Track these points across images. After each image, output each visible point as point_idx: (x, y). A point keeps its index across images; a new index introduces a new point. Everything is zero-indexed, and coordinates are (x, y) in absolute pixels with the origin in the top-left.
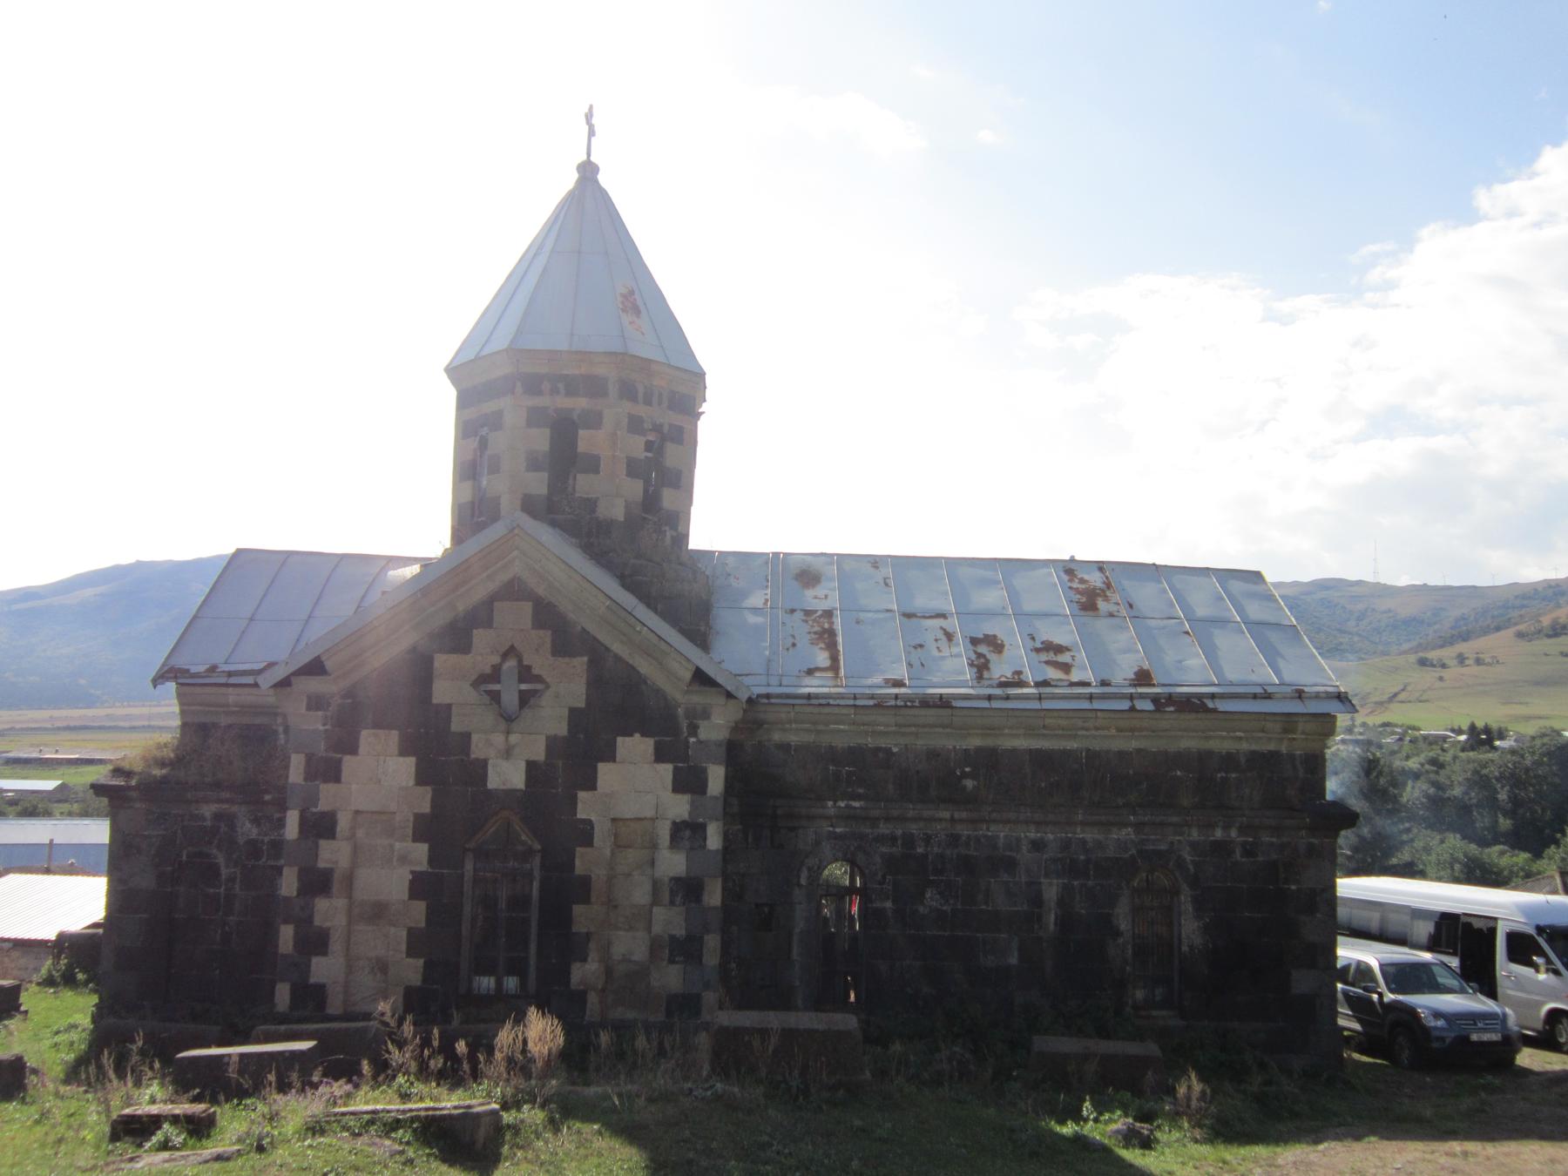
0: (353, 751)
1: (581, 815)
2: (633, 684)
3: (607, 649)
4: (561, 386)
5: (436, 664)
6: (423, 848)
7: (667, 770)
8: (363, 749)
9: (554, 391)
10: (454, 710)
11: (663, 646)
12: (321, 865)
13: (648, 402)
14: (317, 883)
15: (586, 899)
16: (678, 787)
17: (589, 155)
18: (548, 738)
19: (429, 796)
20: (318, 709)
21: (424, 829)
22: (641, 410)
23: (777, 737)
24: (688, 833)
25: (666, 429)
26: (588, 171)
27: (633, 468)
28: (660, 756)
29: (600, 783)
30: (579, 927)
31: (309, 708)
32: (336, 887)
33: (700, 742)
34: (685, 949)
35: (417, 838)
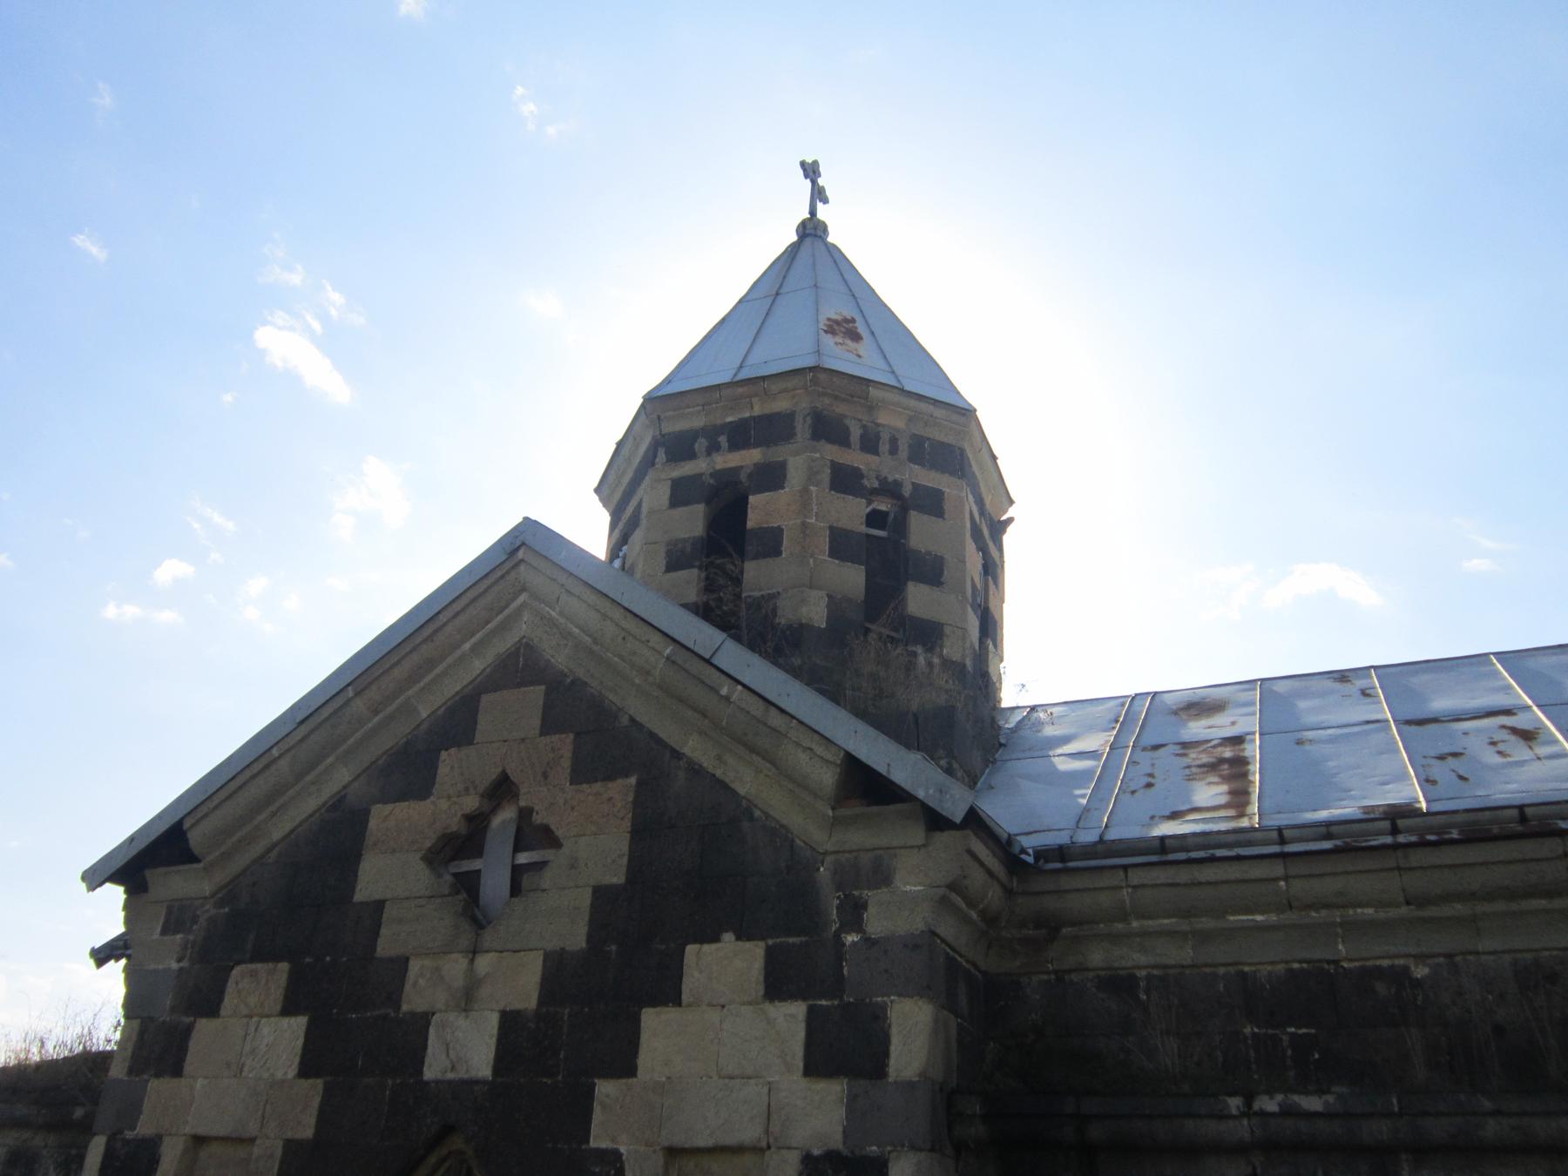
0: (212, 1010)
1: (598, 1140)
2: (723, 817)
3: (676, 755)
4: (723, 440)
5: (373, 823)
7: (791, 1016)
8: (229, 1002)
9: (713, 448)
10: (389, 912)
11: (776, 720)
13: (870, 444)
16: (818, 1064)
18: (548, 956)
19: (316, 1102)
20: (176, 932)
22: (855, 458)
23: (1097, 957)
25: (907, 491)
26: (811, 230)
27: (842, 546)
28: (779, 983)
29: (644, 1060)
33: (869, 942)
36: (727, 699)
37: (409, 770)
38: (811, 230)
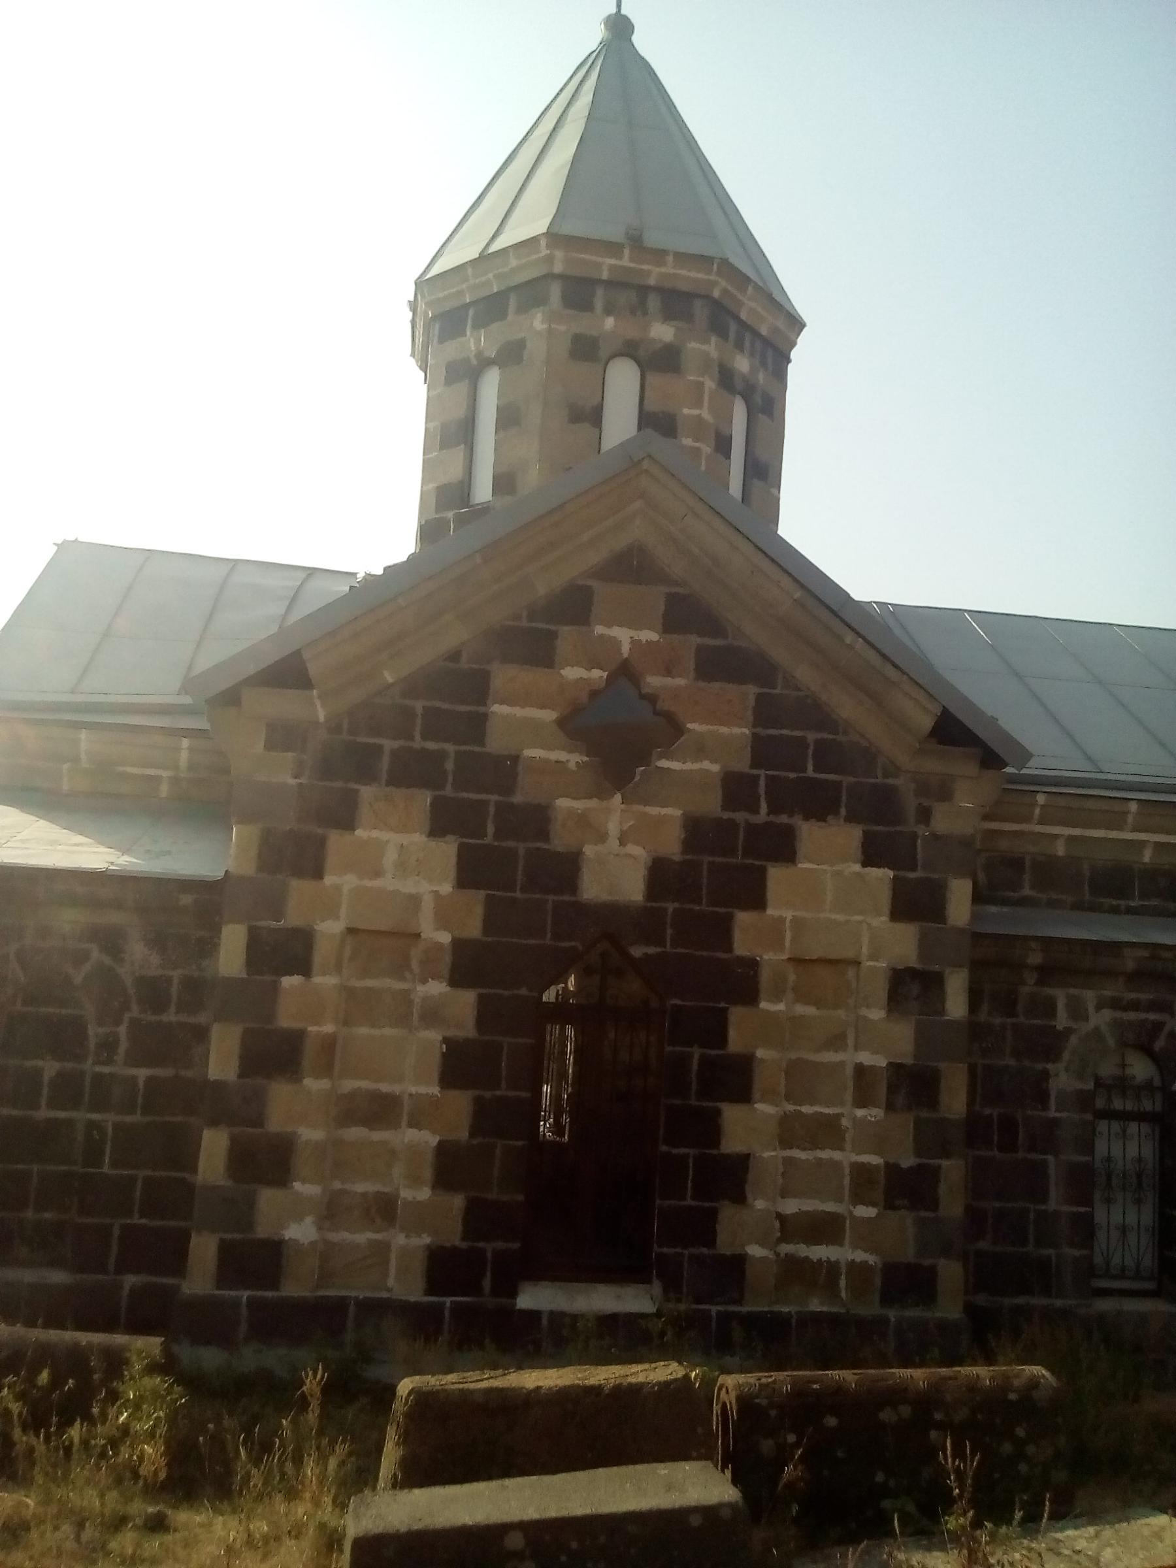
1: (741, 948)
6: (467, 999)
12: (285, 1021)
14: (276, 1054)
15: (744, 1095)
17: (619, 6)
19: (479, 910)
20: (287, 749)
21: (467, 965)
24: (915, 988)
26: (620, 27)
28: (871, 856)
31: (270, 746)
32: (309, 1058)
33: (935, 837)
34: (906, 1188)
35: (458, 979)
36: (850, 647)
37: (531, 643)
38: (620, 27)
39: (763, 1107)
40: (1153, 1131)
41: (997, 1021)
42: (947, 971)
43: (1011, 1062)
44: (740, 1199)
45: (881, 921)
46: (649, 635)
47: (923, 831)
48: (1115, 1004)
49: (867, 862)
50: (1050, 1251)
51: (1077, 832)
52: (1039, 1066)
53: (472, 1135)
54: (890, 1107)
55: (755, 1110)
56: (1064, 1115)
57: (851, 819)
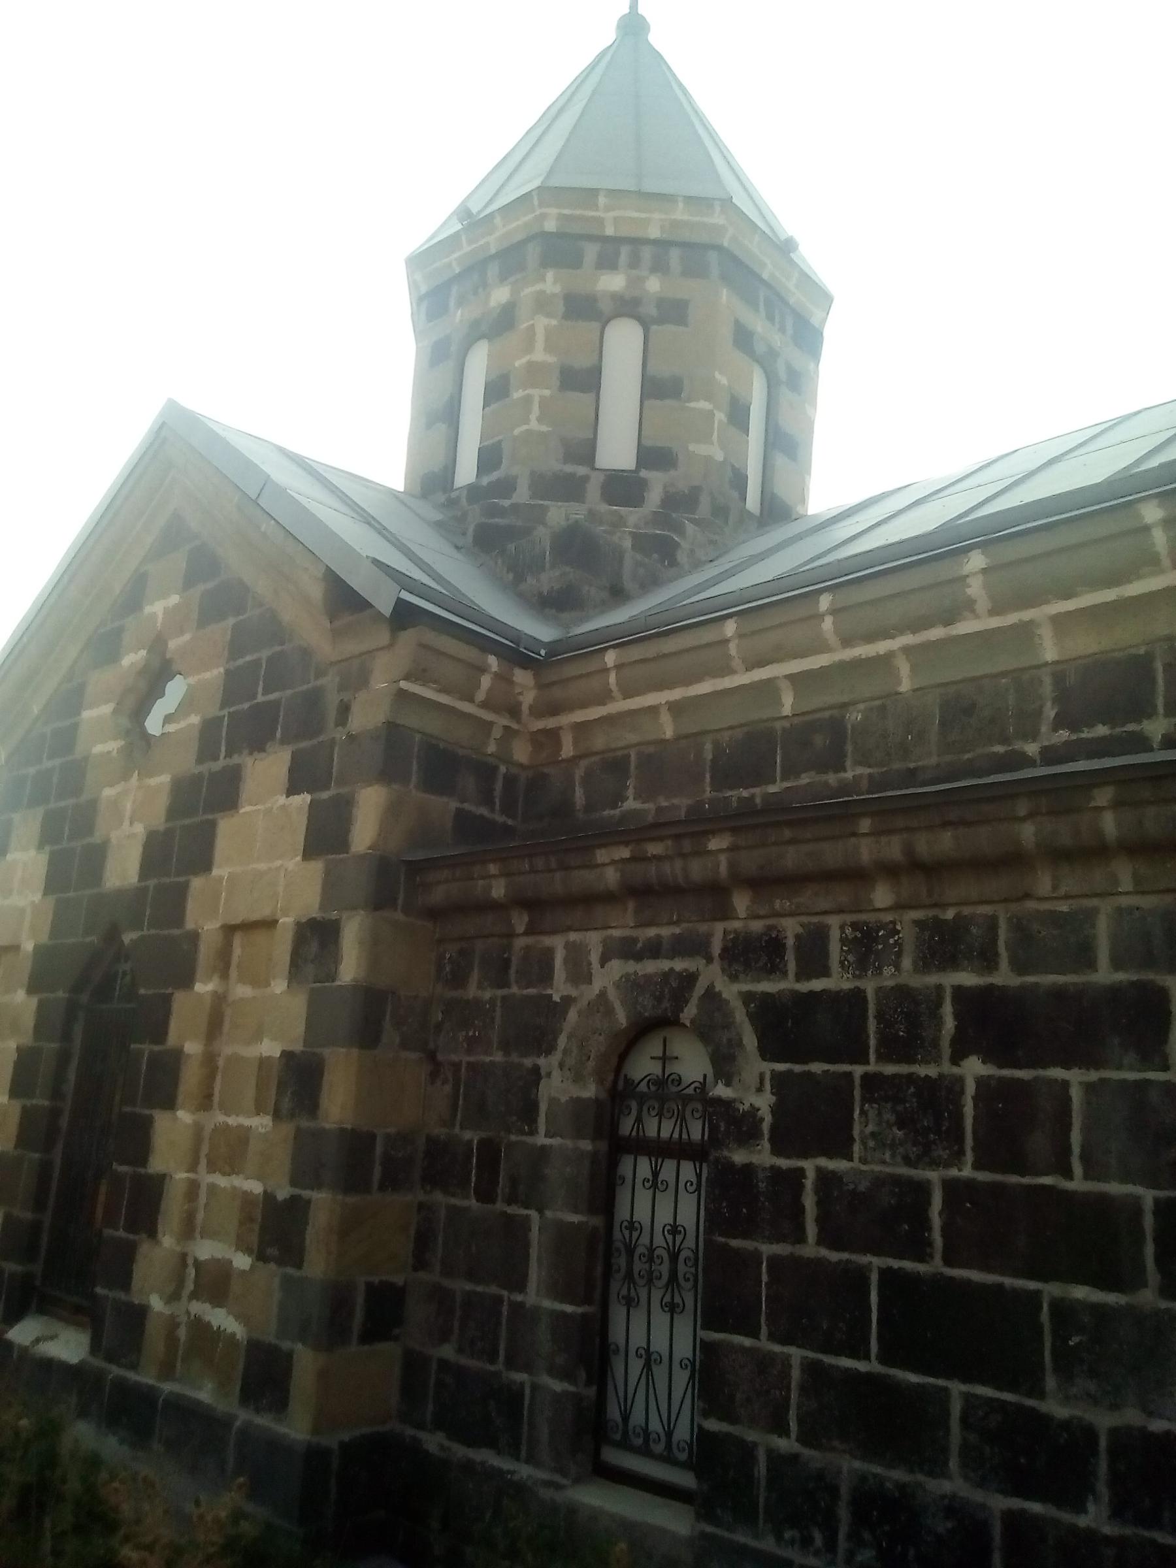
15: (170, 1104)
24: (314, 947)
26: (633, 27)
30: (157, 1164)
33: (351, 737)
38: (633, 27)
39: (184, 1116)
40: (699, 1176)
41: (487, 995)
42: (345, 916)
43: (498, 1057)
44: (152, 1234)
45: (294, 862)
46: (174, 599)
47: (340, 735)
48: (628, 950)
49: (292, 789)
50: (520, 1377)
51: (676, 694)
52: (528, 1062)
53: (16, 1147)
54: (277, 1115)
55: (176, 1119)
56: (555, 1142)
57: (284, 741)
